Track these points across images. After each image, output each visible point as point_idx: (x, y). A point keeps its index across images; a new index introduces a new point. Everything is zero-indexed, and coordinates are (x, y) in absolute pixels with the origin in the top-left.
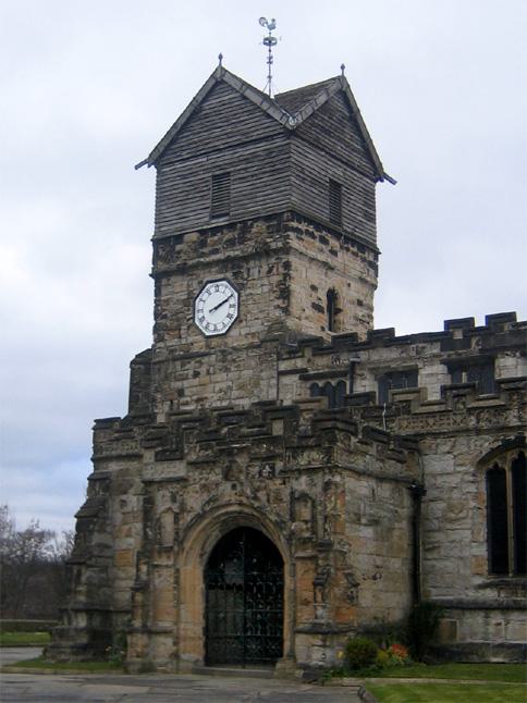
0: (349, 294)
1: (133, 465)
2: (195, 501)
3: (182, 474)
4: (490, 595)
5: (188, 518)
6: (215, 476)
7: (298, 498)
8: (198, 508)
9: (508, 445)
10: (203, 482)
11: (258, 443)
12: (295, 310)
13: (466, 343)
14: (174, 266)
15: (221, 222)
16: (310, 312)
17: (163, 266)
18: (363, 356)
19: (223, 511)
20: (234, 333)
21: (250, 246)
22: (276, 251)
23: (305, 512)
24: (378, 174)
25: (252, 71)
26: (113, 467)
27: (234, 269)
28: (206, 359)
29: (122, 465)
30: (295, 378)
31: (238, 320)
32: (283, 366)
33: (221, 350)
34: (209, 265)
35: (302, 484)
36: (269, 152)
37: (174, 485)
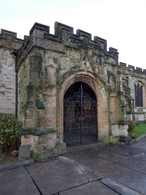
5: (62, 72)
8: (68, 69)
10: (71, 57)
19: (80, 73)
37: (56, 54)
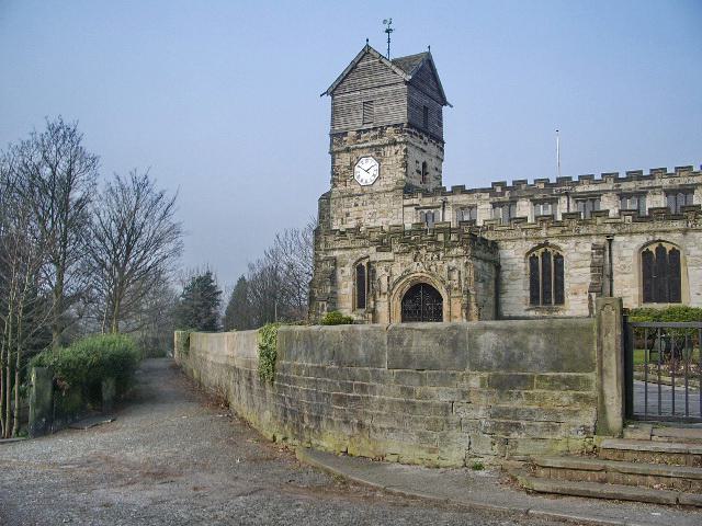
0: (432, 164)
1: (349, 252)
2: (398, 271)
3: (392, 258)
4: (532, 313)
6: (409, 259)
7: (451, 270)
9: (540, 246)
11: (430, 244)
12: (409, 174)
13: (502, 194)
14: (342, 148)
15: (371, 126)
16: (416, 174)
17: (336, 148)
18: (449, 198)
20: (377, 184)
21: (385, 140)
22: (400, 143)
23: (455, 276)
24: (445, 103)
25: (379, 46)
26: (336, 254)
27: (377, 150)
28: (361, 198)
29: (341, 253)
30: (413, 208)
31: (379, 178)
32: (407, 202)
33: (369, 193)
34: (363, 148)
35: (453, 263)
36: (394, 93)
